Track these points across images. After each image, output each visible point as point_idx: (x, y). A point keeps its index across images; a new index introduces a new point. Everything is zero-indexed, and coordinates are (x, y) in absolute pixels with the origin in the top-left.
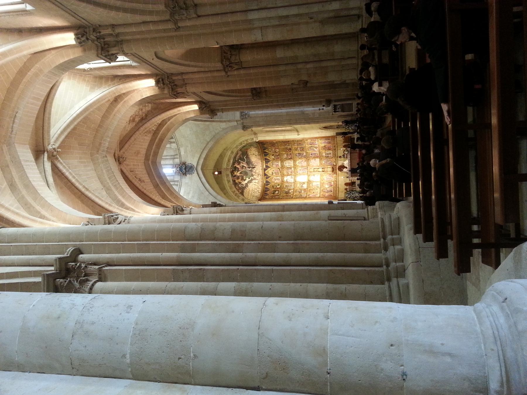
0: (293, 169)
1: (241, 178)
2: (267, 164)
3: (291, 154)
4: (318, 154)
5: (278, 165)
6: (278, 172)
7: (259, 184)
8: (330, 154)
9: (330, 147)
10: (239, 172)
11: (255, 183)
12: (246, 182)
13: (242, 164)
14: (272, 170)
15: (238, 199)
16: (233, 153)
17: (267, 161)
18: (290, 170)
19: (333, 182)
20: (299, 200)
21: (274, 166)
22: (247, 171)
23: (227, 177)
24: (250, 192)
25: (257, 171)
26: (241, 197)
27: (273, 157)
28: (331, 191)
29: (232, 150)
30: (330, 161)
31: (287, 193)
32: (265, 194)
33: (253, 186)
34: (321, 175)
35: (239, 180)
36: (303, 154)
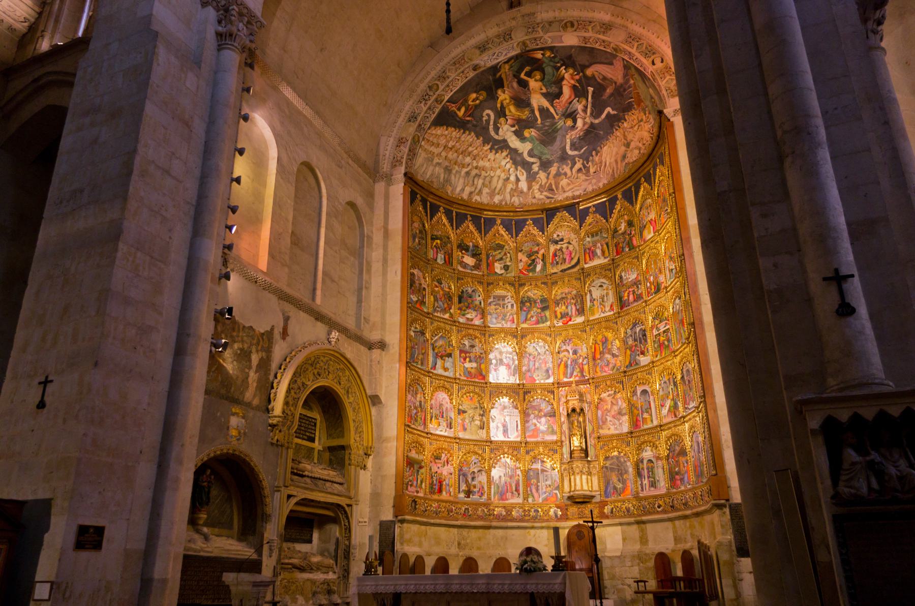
0: (580, 320)
1: (525, 114)
2: (594, 212)
3: (638, 298)
4: (650, 426)
5: (592, 255)
6: (565, 260)
7: (512, 196)
8: (653, 484)
9: (682, 480)
10: (545, 104)
11: (512, 178)
12: (514, 142)
13: (580, 107)
14: (573, 236)
15: (415, 97)
16: (604, 33)
17: (605, 210)
18: (572, 310)
19: (520, 500)
20: (400, 341)
21: (588, 239)
22: (558, 139)
23: (498, 36)
24: (468, 160)
25: (564, 182)
26: (427, 111)
27: (623, 227)
28: (468, 493)
29: (618, 21)
30: (620, 486)
31: (464, 300)
32: (461, 218)
33: (498, 172)
34: (553, 448)
35: (512, 108)
36: (643, 353)
